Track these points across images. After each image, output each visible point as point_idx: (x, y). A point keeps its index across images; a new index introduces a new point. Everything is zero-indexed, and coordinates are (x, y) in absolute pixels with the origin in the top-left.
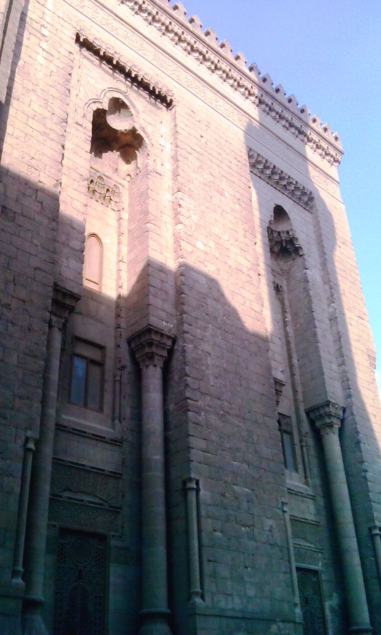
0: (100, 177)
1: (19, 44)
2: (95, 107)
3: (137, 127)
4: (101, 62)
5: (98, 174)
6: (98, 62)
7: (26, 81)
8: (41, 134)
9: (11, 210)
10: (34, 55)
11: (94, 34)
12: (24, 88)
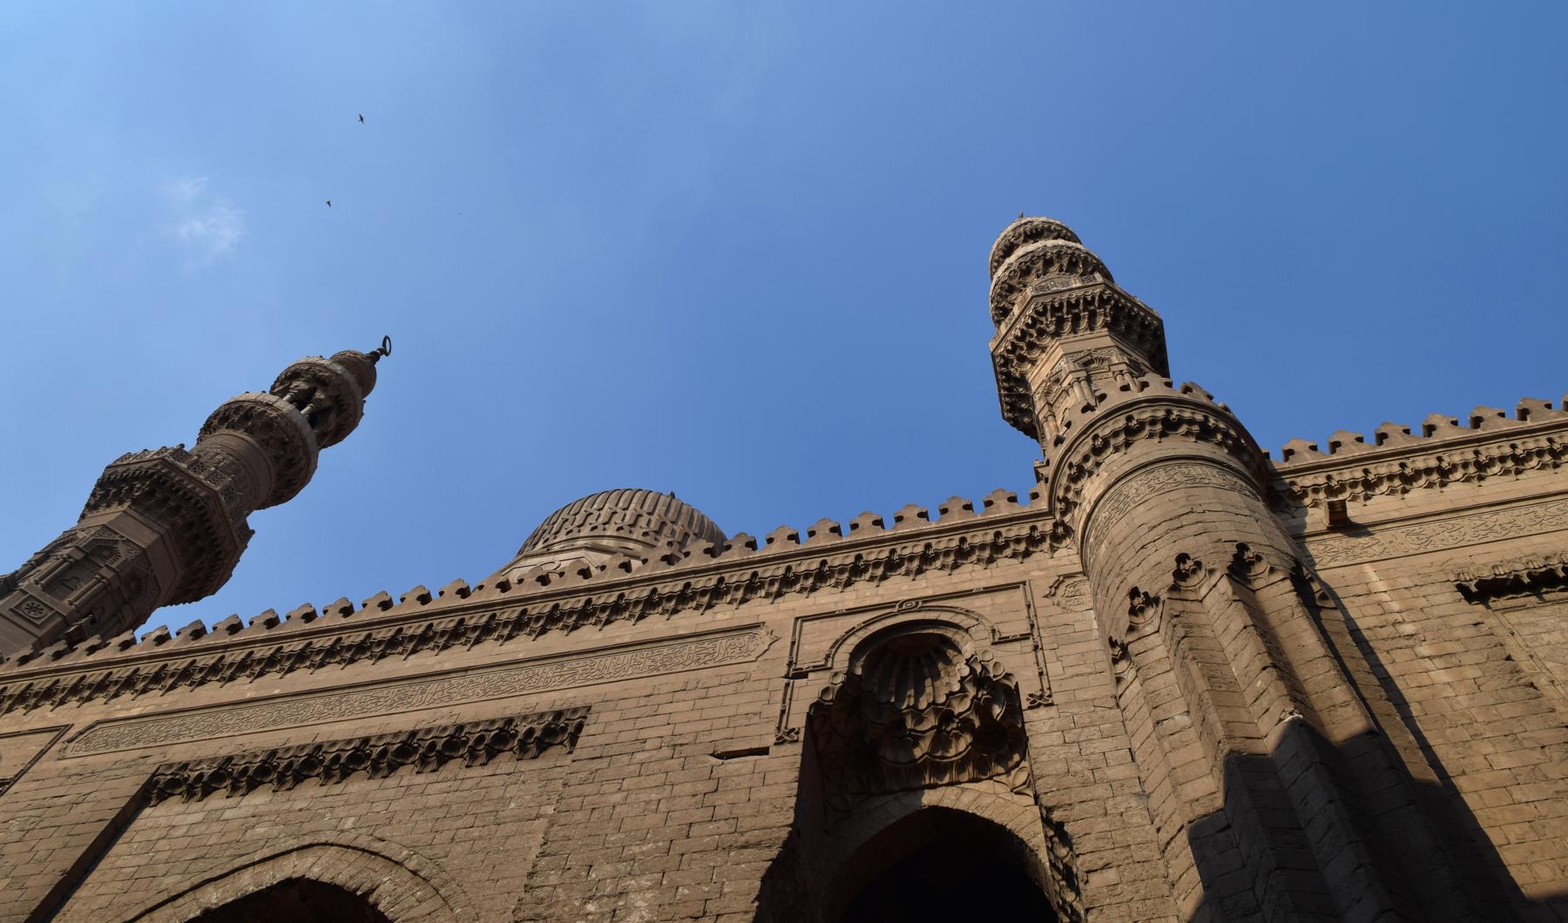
1: (1386, 682)
4: (1539, 595)
6: (1534, 599)
7: (1449, 731)
8: (1557, 800)
11: (1486, 561)
12: (1455, 744)
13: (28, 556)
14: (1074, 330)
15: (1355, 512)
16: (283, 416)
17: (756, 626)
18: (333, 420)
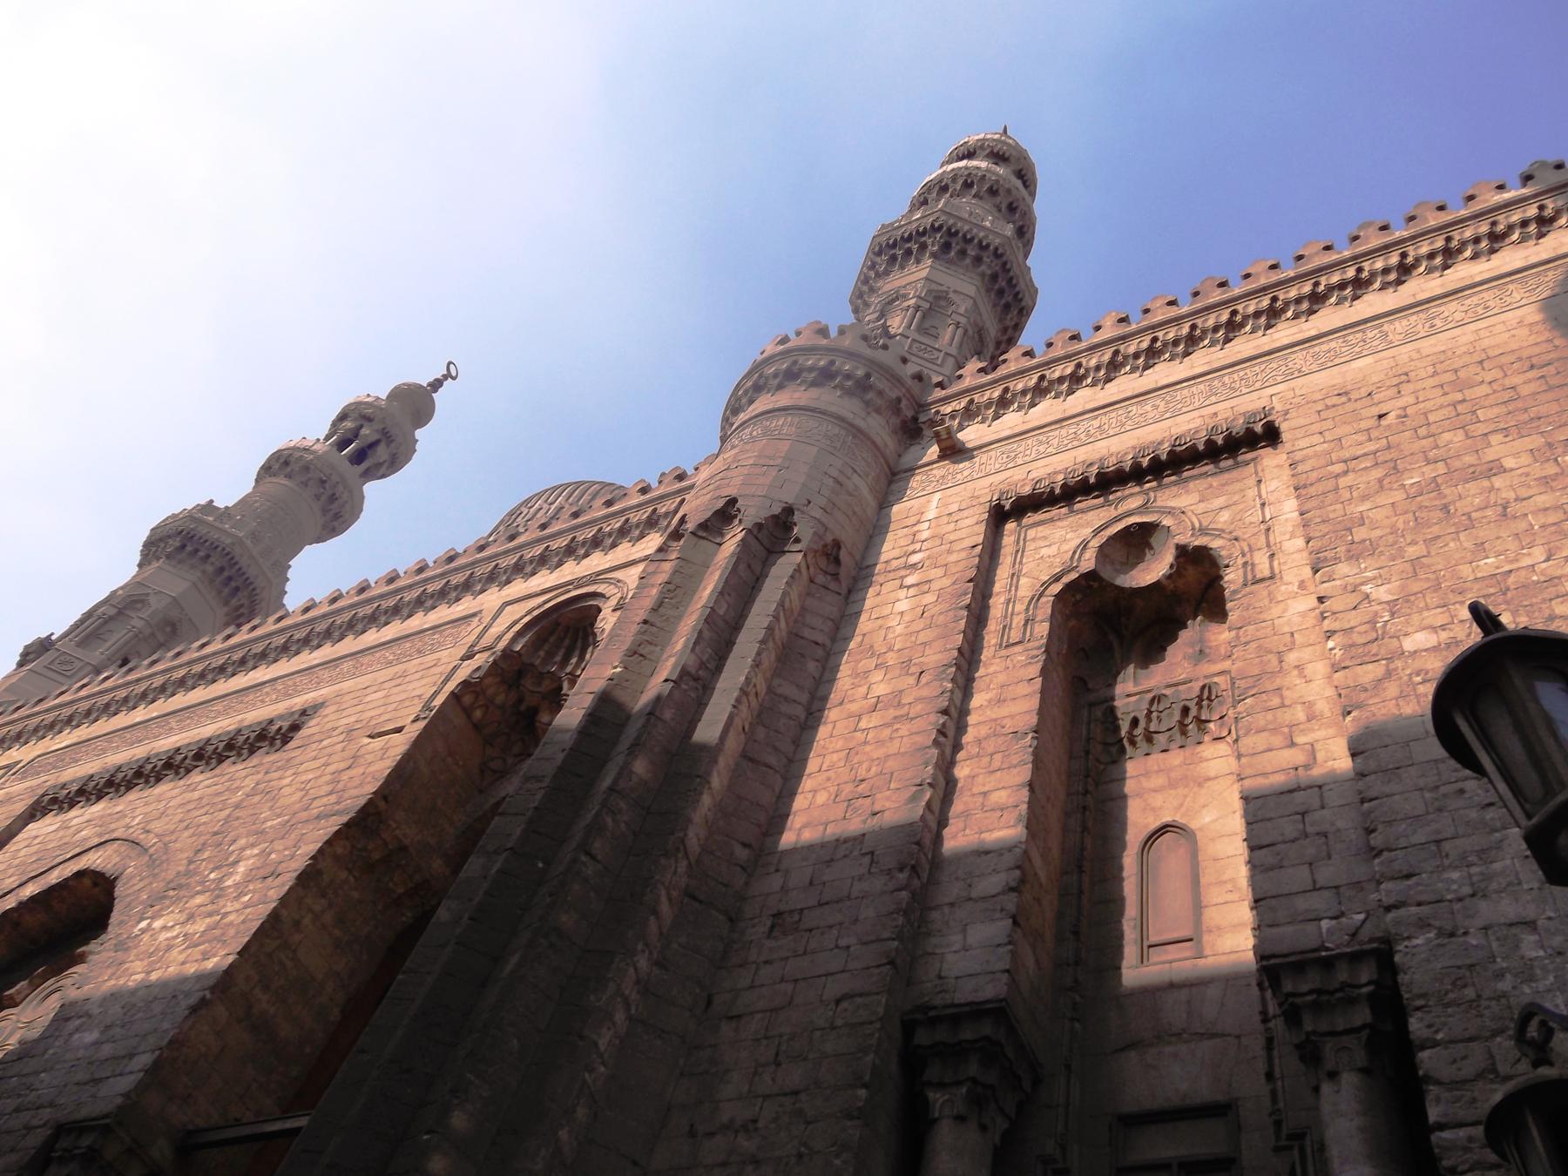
0: (1157, 699)
2: (1057, 588)
3: (1182, 539)
5: (1150, 696)
9: (791, 912)
10: (886, 610)
13: (78, 616)
14: (902, 268)
15: (970, 435)
16: (319, 458)
17: (474, 615)
18: (382, 453)
